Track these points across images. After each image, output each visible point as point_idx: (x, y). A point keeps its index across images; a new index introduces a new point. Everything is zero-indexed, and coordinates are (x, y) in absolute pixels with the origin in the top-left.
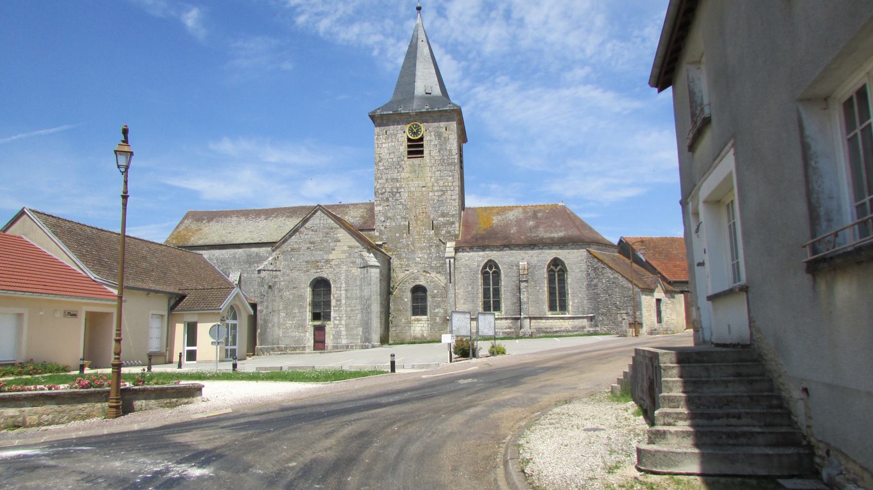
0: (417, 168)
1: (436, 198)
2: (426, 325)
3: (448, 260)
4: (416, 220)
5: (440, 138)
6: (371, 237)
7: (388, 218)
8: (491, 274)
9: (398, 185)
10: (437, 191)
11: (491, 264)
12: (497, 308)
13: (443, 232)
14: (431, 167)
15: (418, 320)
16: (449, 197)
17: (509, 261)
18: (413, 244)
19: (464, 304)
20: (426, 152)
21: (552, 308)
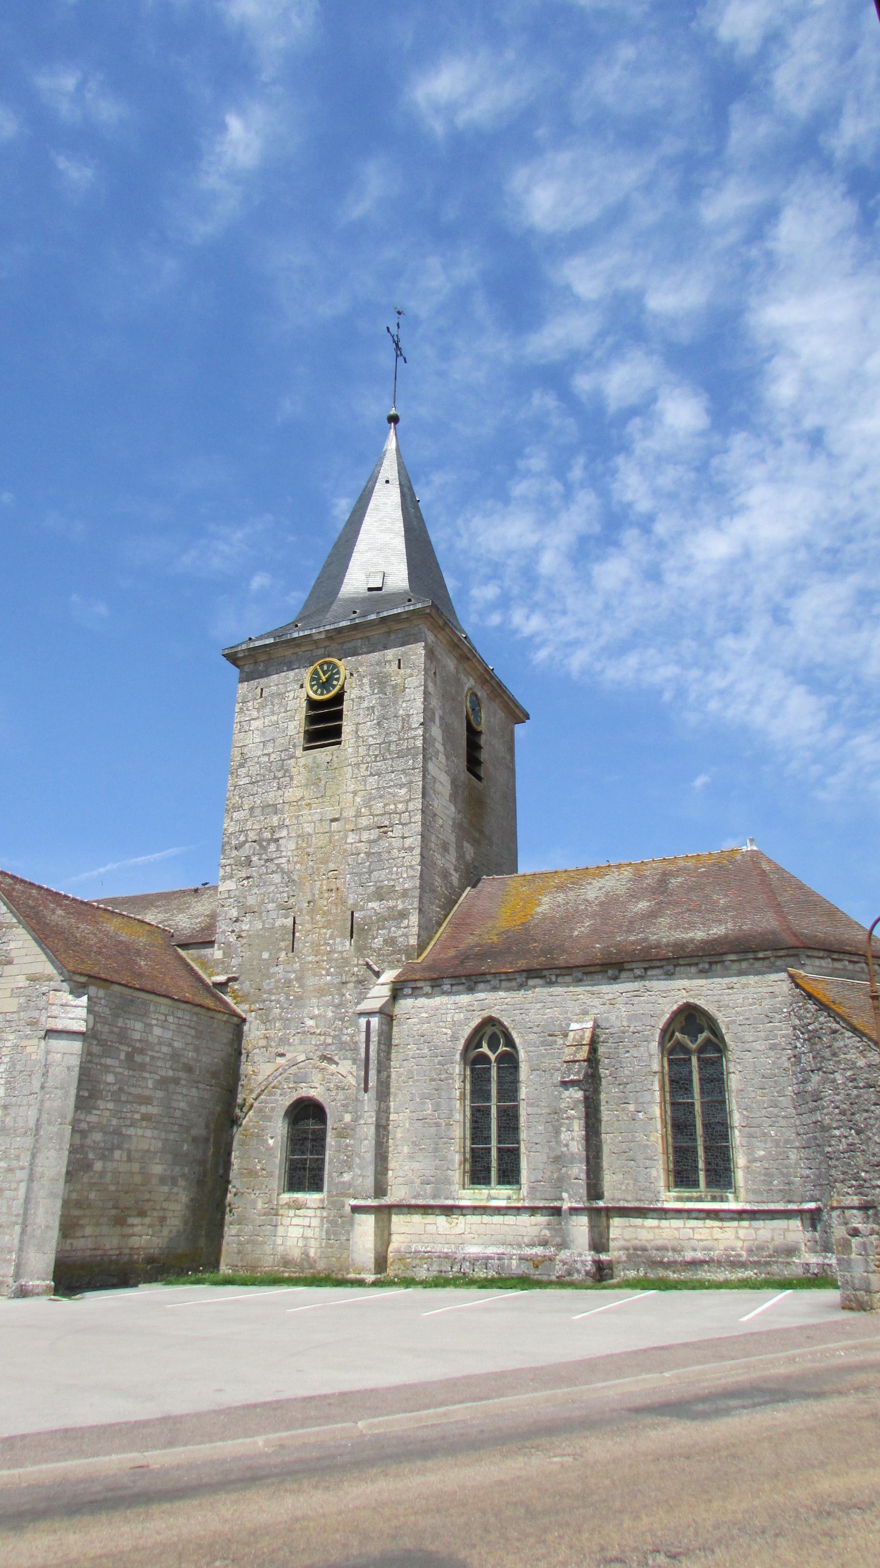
0: (322, 773)
1: (363, 847)
2: (315, 1222)
3: (363, 1021)
4: (312, 912)
5: (382, 691)
6: (204, 965)
7: (246, 910)
8: (490, 1058)
9: (275, 820)
10: (368, 828)
11: (491, 1031)
12: (509, 1175)
13: (378, 942)
14: (357, 765)
15: (298, 1206)
16: (396, 843)
17: (549, 1019)
18: (299, 979)
19: (411, 1157)
20: (347, 727)
21: (682, 1176)
